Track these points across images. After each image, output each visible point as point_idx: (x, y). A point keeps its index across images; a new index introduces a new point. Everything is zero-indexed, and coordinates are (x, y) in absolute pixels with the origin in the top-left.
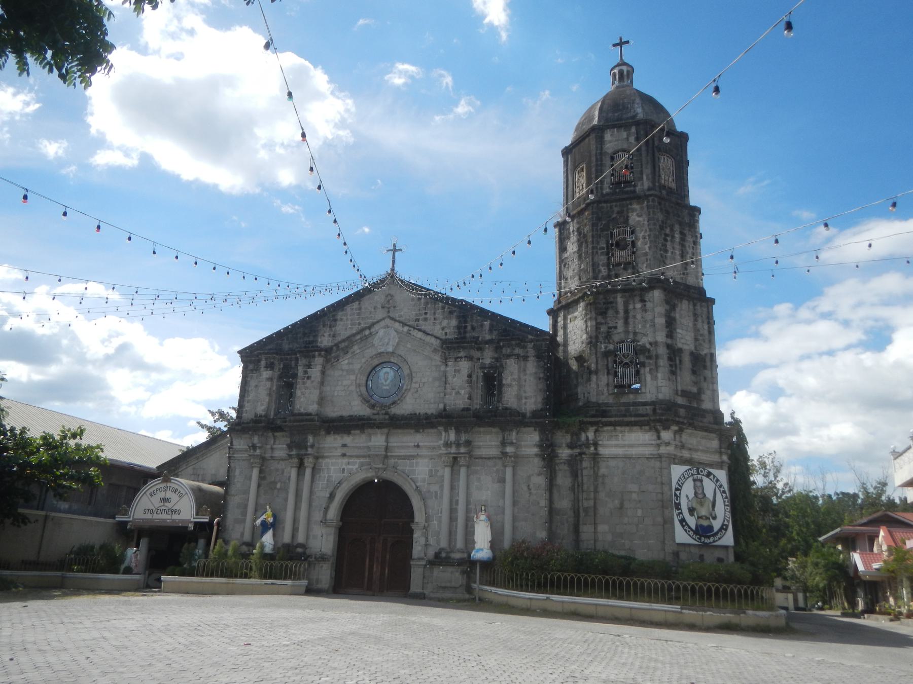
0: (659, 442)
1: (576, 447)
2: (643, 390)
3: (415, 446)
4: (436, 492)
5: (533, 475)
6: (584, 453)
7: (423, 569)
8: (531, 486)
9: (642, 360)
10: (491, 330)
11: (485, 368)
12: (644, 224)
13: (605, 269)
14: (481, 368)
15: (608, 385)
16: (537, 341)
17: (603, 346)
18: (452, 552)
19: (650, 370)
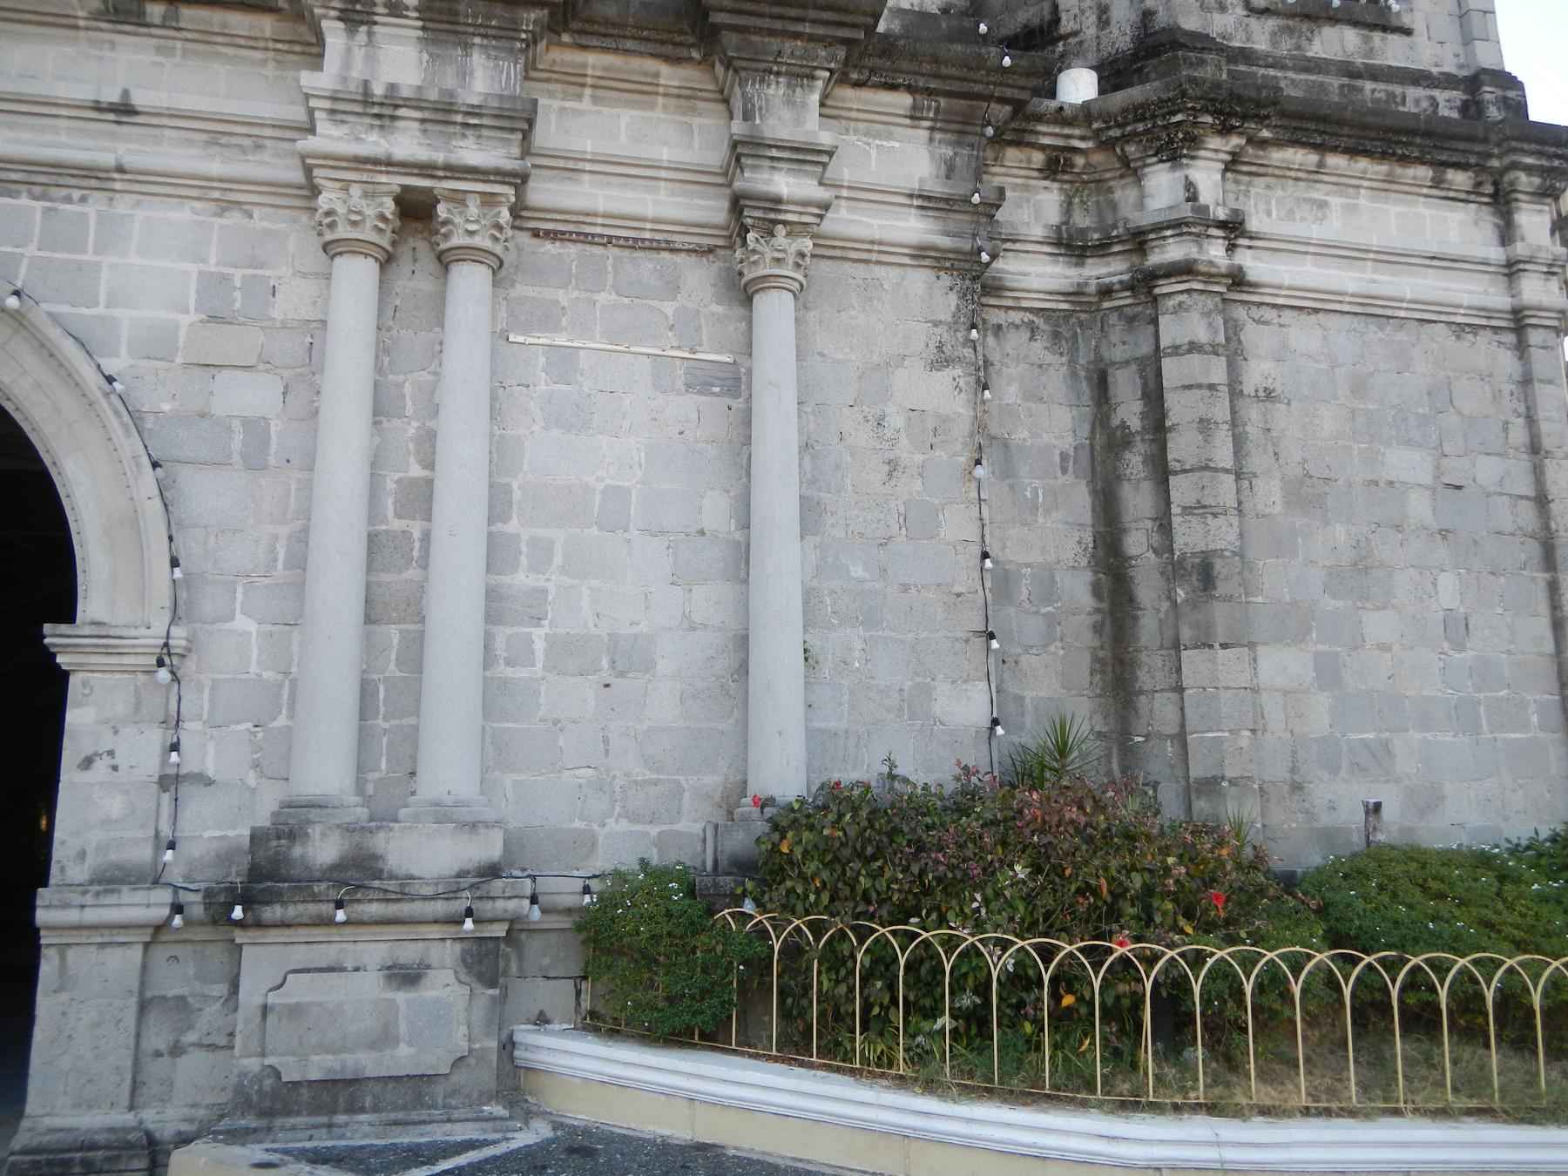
0: (1520, 249)
1: (1102, 249)
2: (1406, 21)
3: (98, 107)
4: (256, 428)
6: (1185, 269)
7: (136, 953)
8: (896, 420)
18: (384, 819)
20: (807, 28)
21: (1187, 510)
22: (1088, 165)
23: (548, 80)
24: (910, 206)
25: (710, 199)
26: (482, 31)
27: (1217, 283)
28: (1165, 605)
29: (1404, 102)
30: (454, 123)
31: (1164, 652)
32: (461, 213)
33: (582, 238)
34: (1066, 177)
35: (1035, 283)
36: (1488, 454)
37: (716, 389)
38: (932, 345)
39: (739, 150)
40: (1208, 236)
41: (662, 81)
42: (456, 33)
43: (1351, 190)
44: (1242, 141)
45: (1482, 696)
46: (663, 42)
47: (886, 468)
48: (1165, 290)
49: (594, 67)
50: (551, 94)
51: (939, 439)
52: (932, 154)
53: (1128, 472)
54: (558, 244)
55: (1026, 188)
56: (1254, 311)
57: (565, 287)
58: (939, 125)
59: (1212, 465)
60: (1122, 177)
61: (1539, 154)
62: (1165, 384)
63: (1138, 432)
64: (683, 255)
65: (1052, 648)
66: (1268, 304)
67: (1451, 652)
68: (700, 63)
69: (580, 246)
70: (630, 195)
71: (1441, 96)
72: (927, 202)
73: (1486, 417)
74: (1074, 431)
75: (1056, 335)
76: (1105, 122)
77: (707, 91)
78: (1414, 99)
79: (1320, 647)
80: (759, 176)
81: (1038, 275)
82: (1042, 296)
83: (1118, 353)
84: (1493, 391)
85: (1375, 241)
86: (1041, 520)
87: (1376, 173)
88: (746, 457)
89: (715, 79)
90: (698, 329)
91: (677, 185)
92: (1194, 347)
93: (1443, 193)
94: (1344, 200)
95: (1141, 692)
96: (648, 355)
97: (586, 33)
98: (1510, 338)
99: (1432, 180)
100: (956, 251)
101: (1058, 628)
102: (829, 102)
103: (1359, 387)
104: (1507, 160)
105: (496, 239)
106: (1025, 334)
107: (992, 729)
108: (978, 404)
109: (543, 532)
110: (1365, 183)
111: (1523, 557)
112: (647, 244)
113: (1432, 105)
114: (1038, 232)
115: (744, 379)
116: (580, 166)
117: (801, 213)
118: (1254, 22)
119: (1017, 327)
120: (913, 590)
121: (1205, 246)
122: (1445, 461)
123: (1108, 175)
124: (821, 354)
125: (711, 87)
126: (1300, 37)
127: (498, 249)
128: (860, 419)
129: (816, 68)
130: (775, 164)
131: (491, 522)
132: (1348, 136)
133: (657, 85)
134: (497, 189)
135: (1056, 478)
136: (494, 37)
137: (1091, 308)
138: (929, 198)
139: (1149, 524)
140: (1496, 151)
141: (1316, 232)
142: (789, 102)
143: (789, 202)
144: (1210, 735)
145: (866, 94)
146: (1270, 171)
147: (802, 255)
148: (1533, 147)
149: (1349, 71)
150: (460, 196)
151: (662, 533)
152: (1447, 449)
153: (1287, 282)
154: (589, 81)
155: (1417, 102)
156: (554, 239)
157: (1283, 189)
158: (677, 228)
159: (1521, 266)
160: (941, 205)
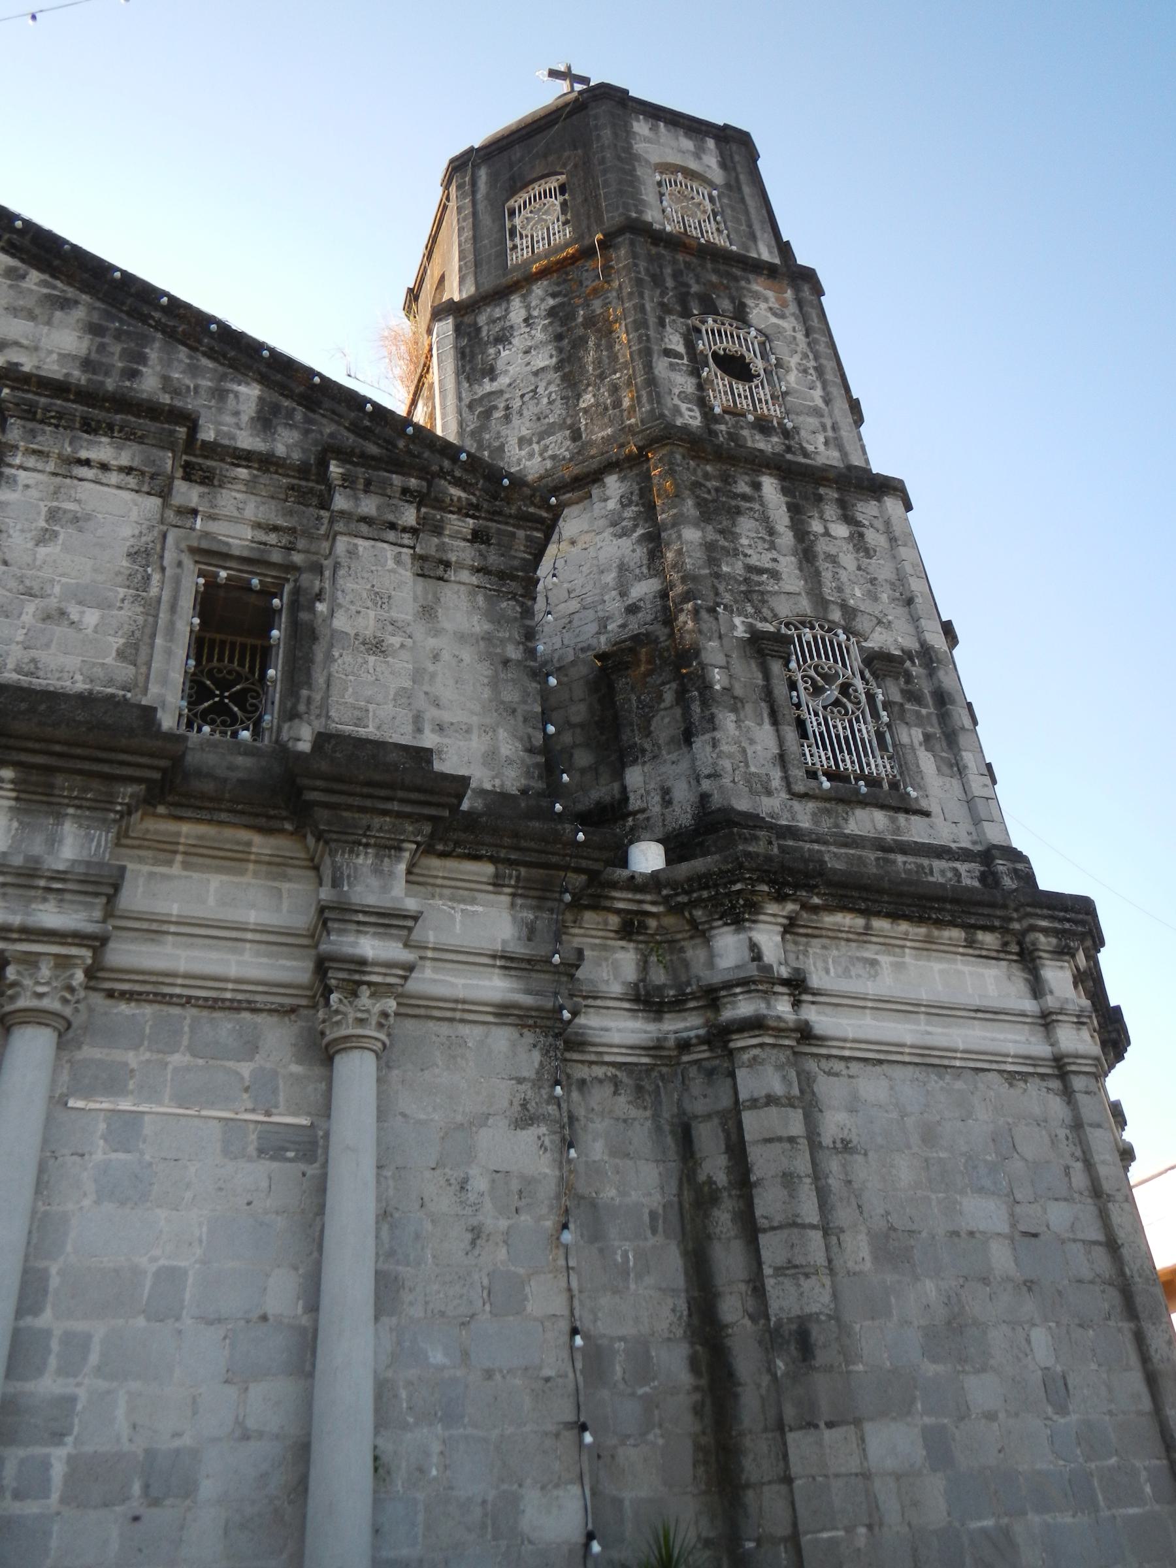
0: (1051, 1002)
1: (677, 1005)
2: (924, 804)
5: (483, 1119)
6: (756, 1024)
8: (480, 1183)
9: (897, 697)
10: (265, 420)
11: (222, 556)
12: (795, 338)
13: (690, 410)
14: (197, 552)
15: (782, 759)
16: (494, 515)
17: (737, 621)
19: (927, 738)
20: (395, 806)
21: (779, 1271)
22: (660, 927)
23: (139, 847)
24: (493, 966)
25: (295, 959)
26: (76, 802)
27: (787, 1037)
28: (766, 1380)
29: (932, 873)
30: (37, 888)
31: (770, 1435)
32: (31, 975)
33: (159, 998)
34: (641, 938)
35: (616, 1038)
36: (1056, 1200)
37: (291, 1154)
38: (516, 1103)
39: (327, 914)
40: (775, 993)
41: (254, 850)
42: (49, 803)
43: (897, 950)
44: (797, 907)
45: (1093, 1466)
46: (257, 815)
47: (469, 1236)
48: (740, 1044)
49: (187, 837)
50: (141, 860)
51: (524, 1202)
52: (514, 918)
53: (718, 1230)
54: (133, 1004)
55: (604, 948)
56: (824, 1064)
57: (136, 1048)
58: (520, 891)
59: (799, 1221)
60: (692, 938)
61: (1052, 918)
62: (747, 1137)
63: (725, 1188)
64: (264, 1015)
65: (651, 1437)
66: (836, 1057)
67: (1055, 1417)
68: (292, 834)
69: (157, 1007)
70: (214, 955)
71: (963, 867)
72: (508, 962)
73: (1047, 1162)
74: (662, 1188)
75: (639, 1089)
76: (674, 889)
77: (297, 858)
78: (940, 871)
79: (927, 1420)
80: (345, 939)
81: (619, 1030)
82: (624, 1051)
83: (699, 1107)
84: (1050, 1136)
85: (924, 995)
86: (633, 1286)
87: (917, 934)
88: (318, 1229)
89: (307, 848)
90: (275, 1091)
91: (263, 947)
92: (771, 1100)
93: (977, 952)
94: (892, 959)
95: (748, 1486)
96: (220, 1119)
97: (181, 805)
98: (1056, 1084)
99: (966, 940)
100: (537, 1009)
101: (656, 1412)
102: (416, 870)
103: (929, 1136)
104: (1025, 923)
105: (65, 1001)
106: (608, 1089)
107: (587, 1546)
108: (563, 1163)
109: (80, 1326)
110: (909, 944)
111: (1106, 1306)
112: (228, 1004)
113: (955, 875)
114: (617, 989)
115: (321, 1142)
116: (165, 928)
117: (385, 975)
118: (797, 805)
119: (601, 1081)
120: (498, 1377)
121: (772, 1002)
122: (1018, 1209)
123: (679, 936)
124: (404, 1115)
125: (302, 855)
126: (837, 817)
127: (67, 1011)
128: (443, 1183)
129: (403, 841)
130: (361, 928)
131: (19, 1313)
132: (887, 902)
133: (250, 853)
134: (74, 951)
135: (646, 1239)
136: (89, 808)
137: (673, 1062)
138: (511, 959)
139: (743, 1287)
140: (1015, 915)
141: (871, 988)
142: (377, 871)
143: (376, 964)
144: (825, 1535)
145: (451, 864)
146: (824, 933)
147: (385, 1015)
148: (1045, 912)
149: (881, 845)
150: (33, 958)
151: (219, 1320)
152: (1019, 1197)
153: (851, 1036)
154: (181, 848)
155: (943, 872)
156: (129, 1000)
157: (837, 949)
158: (260, 988)
159: (1054, 1017)
160: (523, 965)
